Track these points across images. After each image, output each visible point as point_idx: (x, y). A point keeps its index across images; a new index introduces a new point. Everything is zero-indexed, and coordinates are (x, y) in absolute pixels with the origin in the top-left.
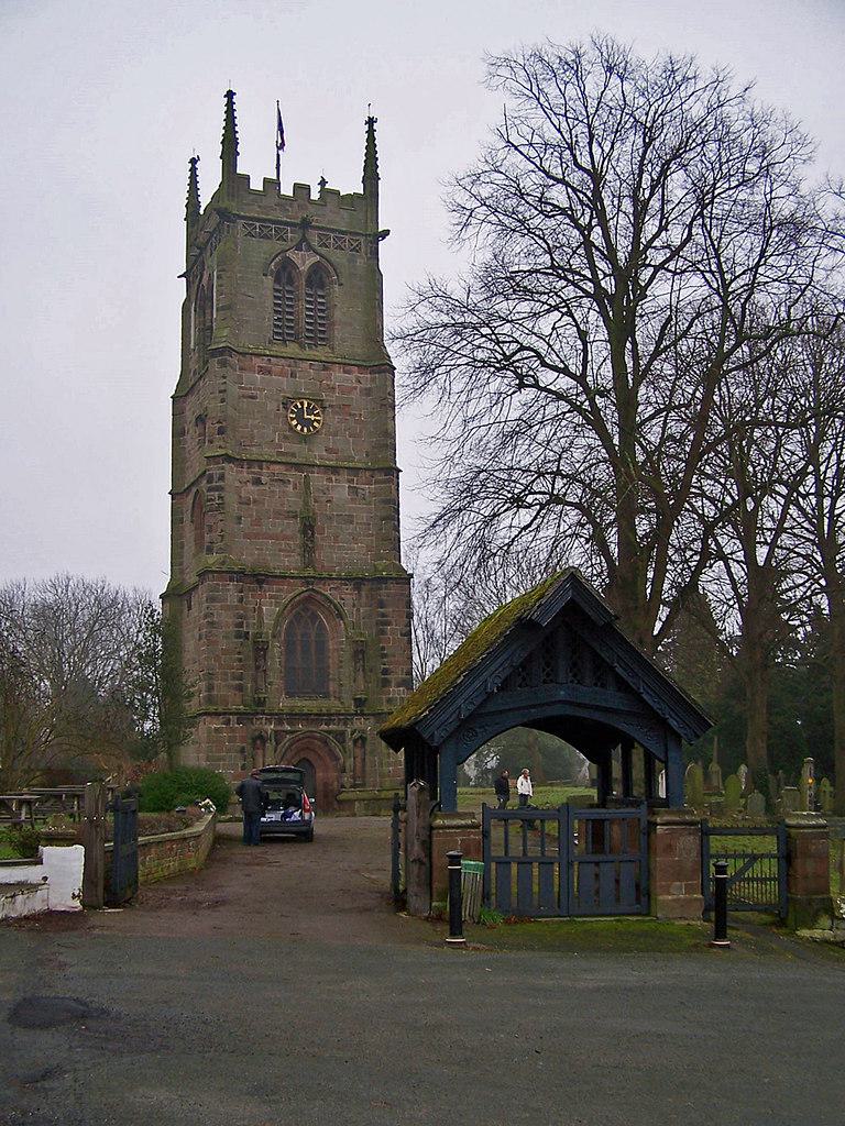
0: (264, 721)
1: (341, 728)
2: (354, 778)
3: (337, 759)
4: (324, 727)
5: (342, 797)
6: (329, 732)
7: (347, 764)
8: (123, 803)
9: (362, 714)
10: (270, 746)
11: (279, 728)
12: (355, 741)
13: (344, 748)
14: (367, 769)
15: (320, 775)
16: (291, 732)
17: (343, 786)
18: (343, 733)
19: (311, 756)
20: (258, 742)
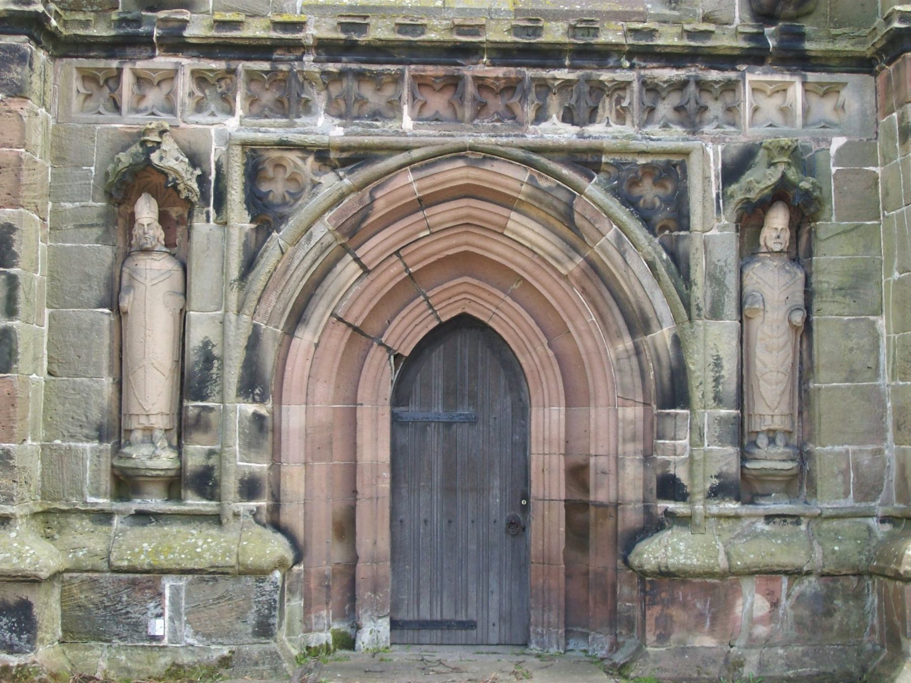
0: (184, 85)
1: (667, 137)
2: (741, 434)
3: (638, 323)
4: (557, 131)
5: (654, 553)
6: (586, 160)
7: (698, 365)
8: (238, 466)
9: (795, 59)
10: (220, 236)
11: (273, 130)
12: (750, 218)
13: (680, 265)
14: (826, 382)
15: (548, 420)
16: (355, 157)
17: (669, 487)
18: (672, 170)
19: (509, 320)
20: (146, 211)
